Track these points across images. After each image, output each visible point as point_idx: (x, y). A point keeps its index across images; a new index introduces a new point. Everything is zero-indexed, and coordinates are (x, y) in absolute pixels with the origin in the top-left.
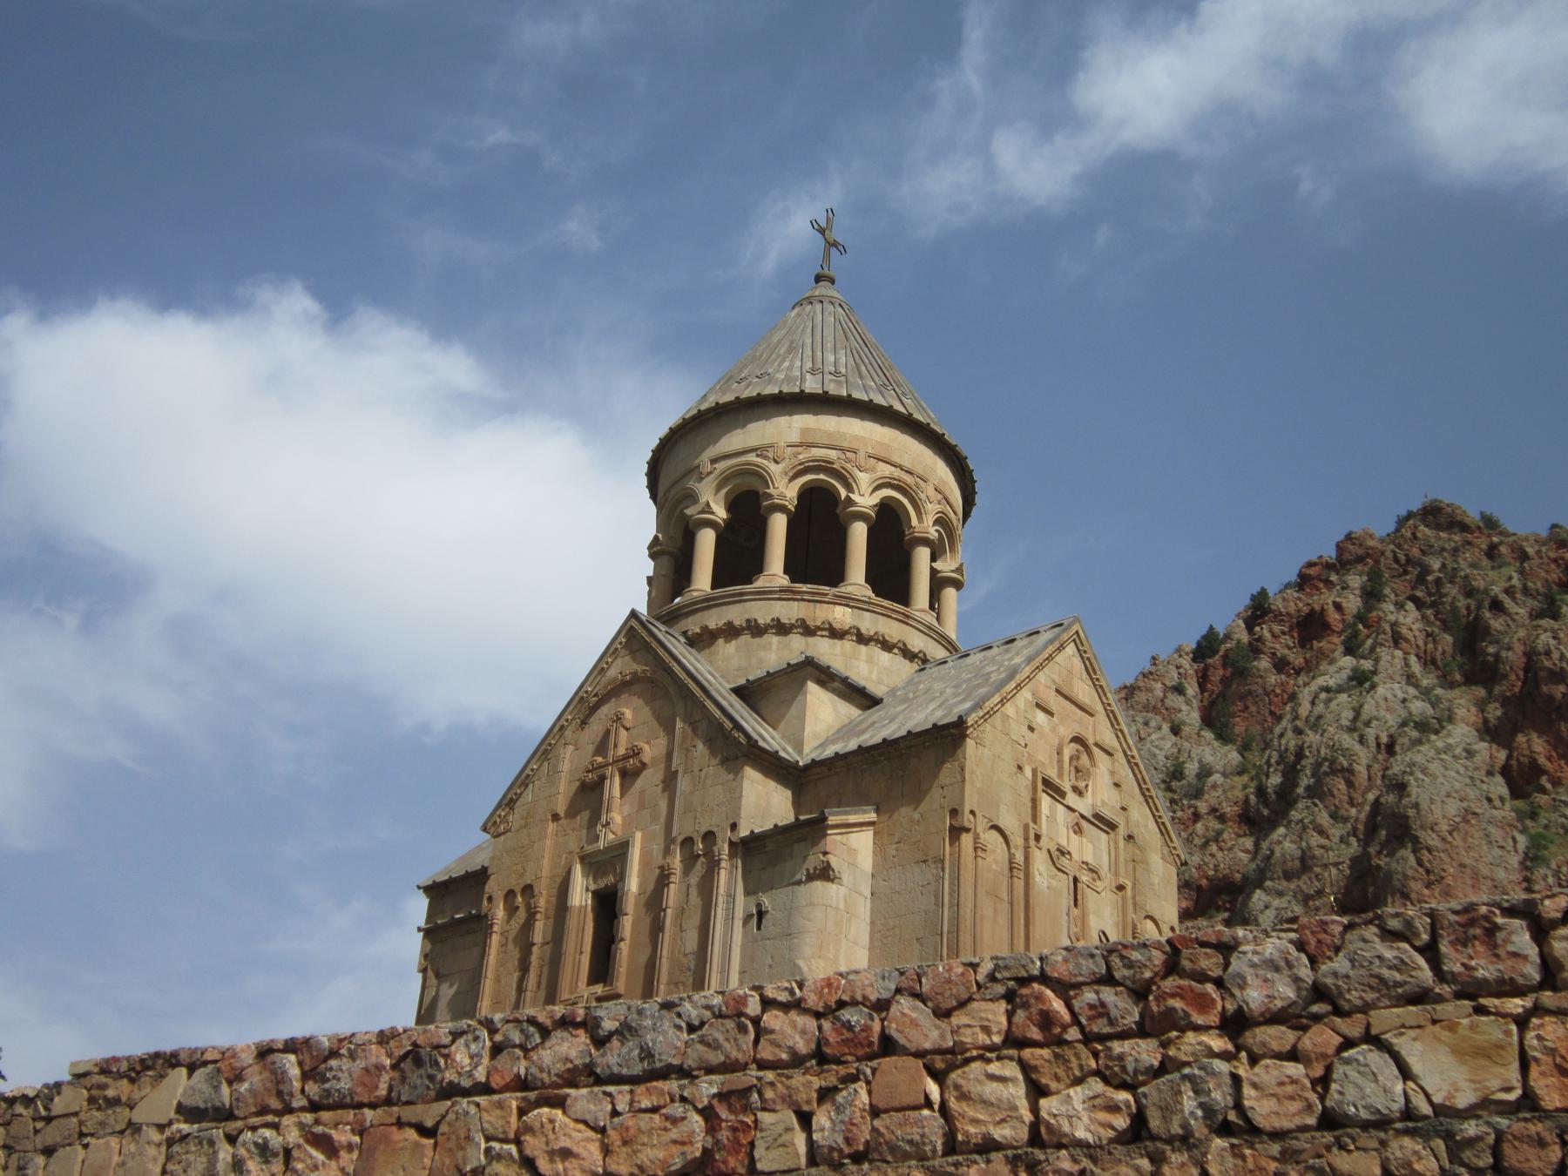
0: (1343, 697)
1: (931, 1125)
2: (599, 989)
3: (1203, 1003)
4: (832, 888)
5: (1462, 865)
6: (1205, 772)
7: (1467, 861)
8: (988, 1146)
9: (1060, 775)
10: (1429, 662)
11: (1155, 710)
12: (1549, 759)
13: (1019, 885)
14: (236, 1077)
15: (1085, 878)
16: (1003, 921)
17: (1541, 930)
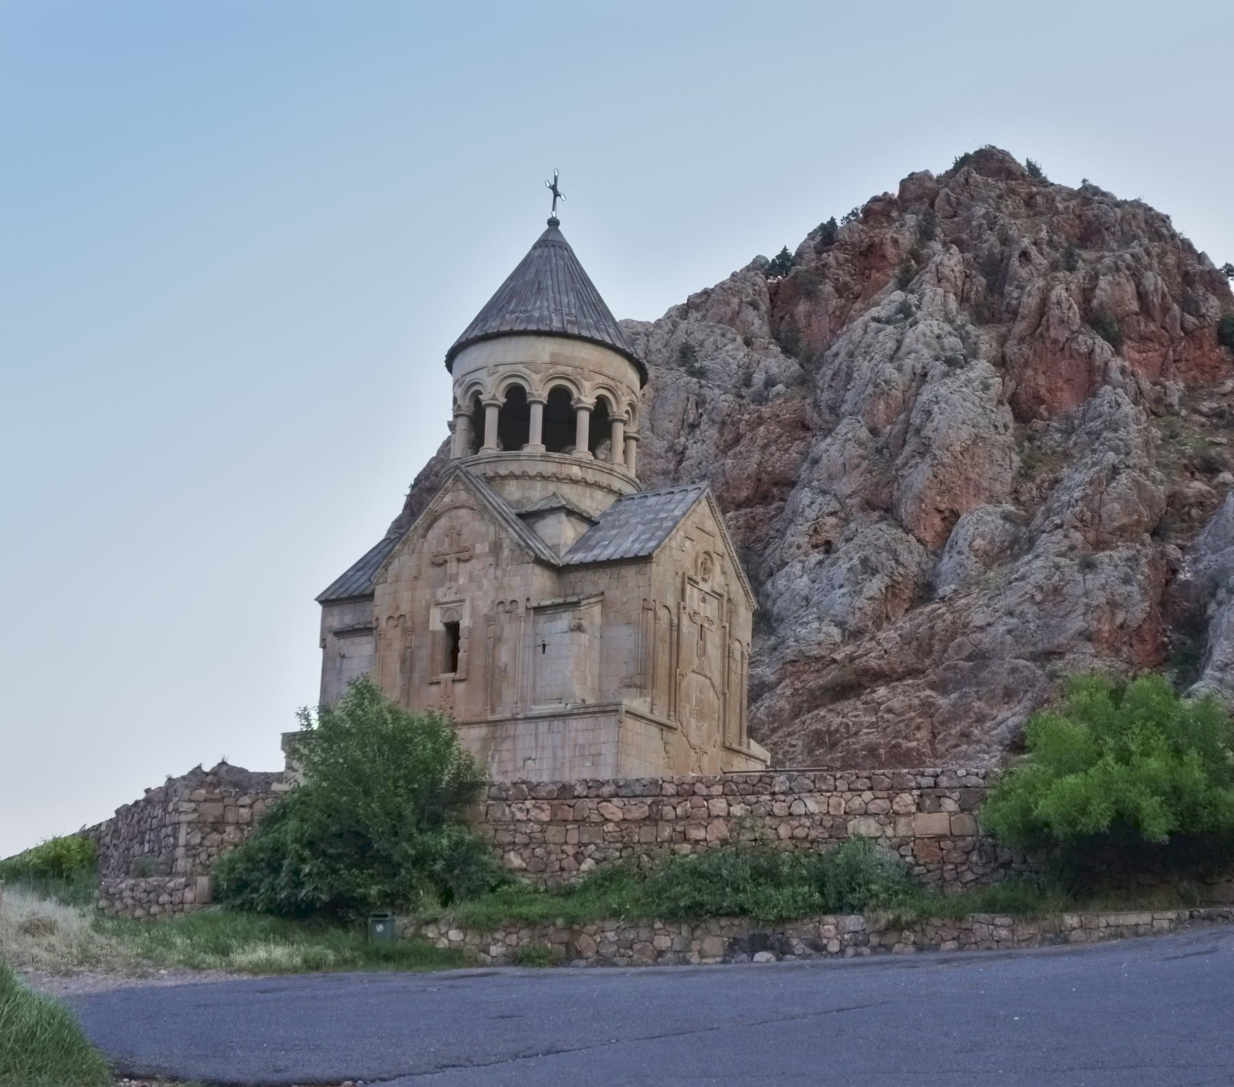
0: (890, 328)
1: (703, 812)
2: (452, 675)
3: (766, 789)
4: (583, 635)
5: (968, 479)
6: (770, 383)
7: (972, 476)
8: (718, 816)
9: (696, 574)
10: (963, 299)
11: (731, 322)
12: (1049, 391)
13: (675, 634)
14: (508, 790)
15: (706, 625)
16: (667, 652)
17: (835, 779)
